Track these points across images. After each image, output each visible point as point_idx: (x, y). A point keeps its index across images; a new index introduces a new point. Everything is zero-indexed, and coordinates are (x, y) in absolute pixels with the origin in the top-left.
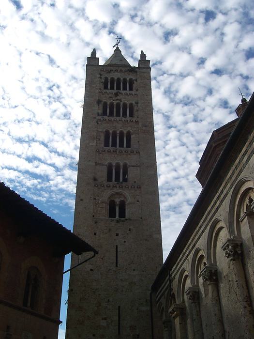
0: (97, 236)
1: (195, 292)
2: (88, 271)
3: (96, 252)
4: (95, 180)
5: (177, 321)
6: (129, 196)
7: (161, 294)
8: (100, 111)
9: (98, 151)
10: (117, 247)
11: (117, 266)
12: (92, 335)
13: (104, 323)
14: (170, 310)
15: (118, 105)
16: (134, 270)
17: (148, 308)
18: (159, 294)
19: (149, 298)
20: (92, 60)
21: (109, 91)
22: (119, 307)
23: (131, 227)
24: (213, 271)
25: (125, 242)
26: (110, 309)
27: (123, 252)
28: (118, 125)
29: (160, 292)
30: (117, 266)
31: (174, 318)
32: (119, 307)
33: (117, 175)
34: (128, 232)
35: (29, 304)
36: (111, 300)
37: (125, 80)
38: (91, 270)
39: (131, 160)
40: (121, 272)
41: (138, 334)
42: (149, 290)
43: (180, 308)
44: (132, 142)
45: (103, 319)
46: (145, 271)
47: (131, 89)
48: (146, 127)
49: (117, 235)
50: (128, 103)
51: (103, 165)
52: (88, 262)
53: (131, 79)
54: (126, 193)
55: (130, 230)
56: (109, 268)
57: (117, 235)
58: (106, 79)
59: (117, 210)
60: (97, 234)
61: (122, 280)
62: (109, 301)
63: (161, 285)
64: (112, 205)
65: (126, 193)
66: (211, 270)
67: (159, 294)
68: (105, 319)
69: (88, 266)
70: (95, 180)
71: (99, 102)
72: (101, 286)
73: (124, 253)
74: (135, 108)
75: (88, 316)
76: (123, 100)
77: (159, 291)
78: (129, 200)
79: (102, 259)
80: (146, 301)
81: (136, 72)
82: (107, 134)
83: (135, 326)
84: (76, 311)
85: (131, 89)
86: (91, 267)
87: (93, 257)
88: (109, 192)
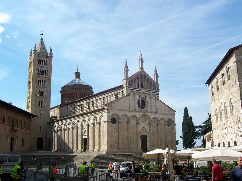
3: (38, 117)
4: (36, 95)
6: (43, 100)
8: (37, 73)
9: (36, 87)
15: (42, 70)
20: (35, 50)
21: (40, 65)
28: (42, 78)
33: (41, 93)
37: (45, 61)
39: (45, 90)
44: (45, 84)
47: (46, 65)
48: (49, 79)
50: (45, 70)
51: (37, 91)
53: (46, 61)
54: (43, 99)
58: (39, 60)
59: (40, 103)
64: (39, 102)
65: (43, 99)
70: (36, 95)
71: (37, 69)
74: (47, 72)
76: (44, 69)
78: (43, 101)
81: (48, 58)
82: (39, 80)
85: (46, 65)
88: (39, 99)
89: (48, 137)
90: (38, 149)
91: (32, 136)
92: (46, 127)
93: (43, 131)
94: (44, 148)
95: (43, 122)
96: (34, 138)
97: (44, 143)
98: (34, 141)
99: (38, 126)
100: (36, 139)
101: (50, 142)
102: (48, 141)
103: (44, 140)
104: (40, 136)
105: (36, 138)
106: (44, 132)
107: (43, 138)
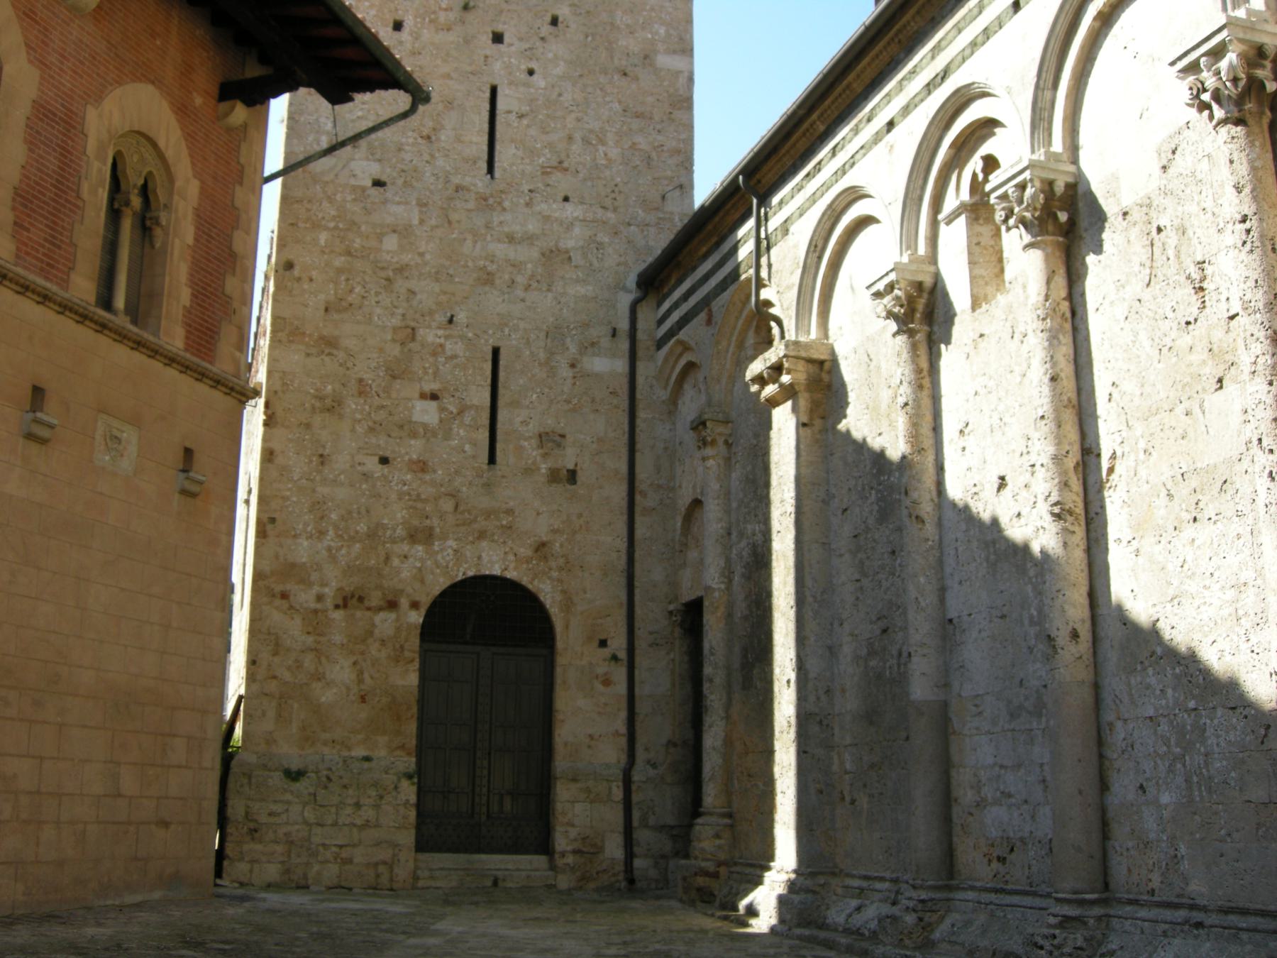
0: (405, 35)
1: (919, 286)
2: (364, 189)
3: (419, 96)
5: (784, 422)
7: (693, 301)
10: (494, 91)
11: (491, 169)
12: (376, 459)
13: (426, 413)
14: (757, 367)
16: (566, 199)
17: (621, 366)
18: (676, 305)
19: (624, 325)
22: (496, 352)
23: (563, 12)
24: (1059, 188)
25: (531, 72)
26: (454, 357)
27: (521, 116)
29: (686, 297)
30: (491, 169)
31: (773, 402)
32: (496, 352)
34: (546, 29)
35: (120, 302)
36: (461, 317)
38: (378, 183)
40: (507, 204)
41: (571, 467)
42: (625, 289)
43: (810, 361)
45: (423, 396)
46: (615, 210)
49: (498, 38)
52: (363, 143)
55: (554, 21)
56: (456, 180)
57: (498, 38)
60: (409, 23)
61: (511, 239)
62: (451, 321)
63: (694, 269)
66: (1051, 184)
67: (676, 305)
68: (434, 397)
69: (361, 166)
72: (422, 255)
73: (525, 122)
75: (361, 381)
77: (677, 294)
79: (429, 137)
80: (614, 333)
83: (563, 436)
84: (308, 355)
86: (375, 170)
87: (405, 115)
89: (651, 572)
90: (433, 833)
91: (303, 551)
92: (608, 365)
93: (550, 440)
94: (580, 814)
95: (554, 256)
96: (344, 602)
97: (585, 720)
98: (341, 672)
99: (430, 335)
100: (385, 622)
101: (714, 698)
102: (659, 674)
103: (574, 651)
104: (494, 561)
105: (392, 605)
106: (572, 476)
107: (547, 593)
